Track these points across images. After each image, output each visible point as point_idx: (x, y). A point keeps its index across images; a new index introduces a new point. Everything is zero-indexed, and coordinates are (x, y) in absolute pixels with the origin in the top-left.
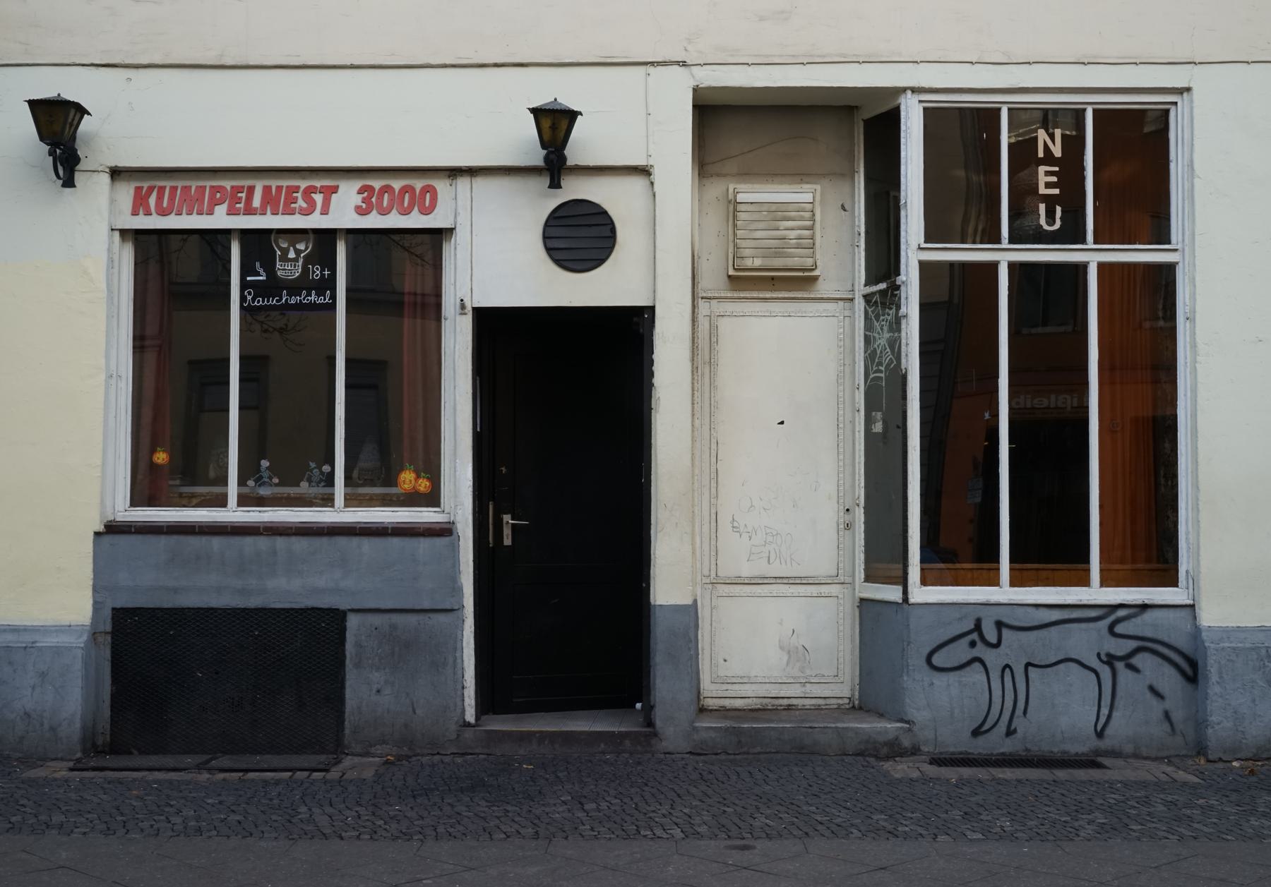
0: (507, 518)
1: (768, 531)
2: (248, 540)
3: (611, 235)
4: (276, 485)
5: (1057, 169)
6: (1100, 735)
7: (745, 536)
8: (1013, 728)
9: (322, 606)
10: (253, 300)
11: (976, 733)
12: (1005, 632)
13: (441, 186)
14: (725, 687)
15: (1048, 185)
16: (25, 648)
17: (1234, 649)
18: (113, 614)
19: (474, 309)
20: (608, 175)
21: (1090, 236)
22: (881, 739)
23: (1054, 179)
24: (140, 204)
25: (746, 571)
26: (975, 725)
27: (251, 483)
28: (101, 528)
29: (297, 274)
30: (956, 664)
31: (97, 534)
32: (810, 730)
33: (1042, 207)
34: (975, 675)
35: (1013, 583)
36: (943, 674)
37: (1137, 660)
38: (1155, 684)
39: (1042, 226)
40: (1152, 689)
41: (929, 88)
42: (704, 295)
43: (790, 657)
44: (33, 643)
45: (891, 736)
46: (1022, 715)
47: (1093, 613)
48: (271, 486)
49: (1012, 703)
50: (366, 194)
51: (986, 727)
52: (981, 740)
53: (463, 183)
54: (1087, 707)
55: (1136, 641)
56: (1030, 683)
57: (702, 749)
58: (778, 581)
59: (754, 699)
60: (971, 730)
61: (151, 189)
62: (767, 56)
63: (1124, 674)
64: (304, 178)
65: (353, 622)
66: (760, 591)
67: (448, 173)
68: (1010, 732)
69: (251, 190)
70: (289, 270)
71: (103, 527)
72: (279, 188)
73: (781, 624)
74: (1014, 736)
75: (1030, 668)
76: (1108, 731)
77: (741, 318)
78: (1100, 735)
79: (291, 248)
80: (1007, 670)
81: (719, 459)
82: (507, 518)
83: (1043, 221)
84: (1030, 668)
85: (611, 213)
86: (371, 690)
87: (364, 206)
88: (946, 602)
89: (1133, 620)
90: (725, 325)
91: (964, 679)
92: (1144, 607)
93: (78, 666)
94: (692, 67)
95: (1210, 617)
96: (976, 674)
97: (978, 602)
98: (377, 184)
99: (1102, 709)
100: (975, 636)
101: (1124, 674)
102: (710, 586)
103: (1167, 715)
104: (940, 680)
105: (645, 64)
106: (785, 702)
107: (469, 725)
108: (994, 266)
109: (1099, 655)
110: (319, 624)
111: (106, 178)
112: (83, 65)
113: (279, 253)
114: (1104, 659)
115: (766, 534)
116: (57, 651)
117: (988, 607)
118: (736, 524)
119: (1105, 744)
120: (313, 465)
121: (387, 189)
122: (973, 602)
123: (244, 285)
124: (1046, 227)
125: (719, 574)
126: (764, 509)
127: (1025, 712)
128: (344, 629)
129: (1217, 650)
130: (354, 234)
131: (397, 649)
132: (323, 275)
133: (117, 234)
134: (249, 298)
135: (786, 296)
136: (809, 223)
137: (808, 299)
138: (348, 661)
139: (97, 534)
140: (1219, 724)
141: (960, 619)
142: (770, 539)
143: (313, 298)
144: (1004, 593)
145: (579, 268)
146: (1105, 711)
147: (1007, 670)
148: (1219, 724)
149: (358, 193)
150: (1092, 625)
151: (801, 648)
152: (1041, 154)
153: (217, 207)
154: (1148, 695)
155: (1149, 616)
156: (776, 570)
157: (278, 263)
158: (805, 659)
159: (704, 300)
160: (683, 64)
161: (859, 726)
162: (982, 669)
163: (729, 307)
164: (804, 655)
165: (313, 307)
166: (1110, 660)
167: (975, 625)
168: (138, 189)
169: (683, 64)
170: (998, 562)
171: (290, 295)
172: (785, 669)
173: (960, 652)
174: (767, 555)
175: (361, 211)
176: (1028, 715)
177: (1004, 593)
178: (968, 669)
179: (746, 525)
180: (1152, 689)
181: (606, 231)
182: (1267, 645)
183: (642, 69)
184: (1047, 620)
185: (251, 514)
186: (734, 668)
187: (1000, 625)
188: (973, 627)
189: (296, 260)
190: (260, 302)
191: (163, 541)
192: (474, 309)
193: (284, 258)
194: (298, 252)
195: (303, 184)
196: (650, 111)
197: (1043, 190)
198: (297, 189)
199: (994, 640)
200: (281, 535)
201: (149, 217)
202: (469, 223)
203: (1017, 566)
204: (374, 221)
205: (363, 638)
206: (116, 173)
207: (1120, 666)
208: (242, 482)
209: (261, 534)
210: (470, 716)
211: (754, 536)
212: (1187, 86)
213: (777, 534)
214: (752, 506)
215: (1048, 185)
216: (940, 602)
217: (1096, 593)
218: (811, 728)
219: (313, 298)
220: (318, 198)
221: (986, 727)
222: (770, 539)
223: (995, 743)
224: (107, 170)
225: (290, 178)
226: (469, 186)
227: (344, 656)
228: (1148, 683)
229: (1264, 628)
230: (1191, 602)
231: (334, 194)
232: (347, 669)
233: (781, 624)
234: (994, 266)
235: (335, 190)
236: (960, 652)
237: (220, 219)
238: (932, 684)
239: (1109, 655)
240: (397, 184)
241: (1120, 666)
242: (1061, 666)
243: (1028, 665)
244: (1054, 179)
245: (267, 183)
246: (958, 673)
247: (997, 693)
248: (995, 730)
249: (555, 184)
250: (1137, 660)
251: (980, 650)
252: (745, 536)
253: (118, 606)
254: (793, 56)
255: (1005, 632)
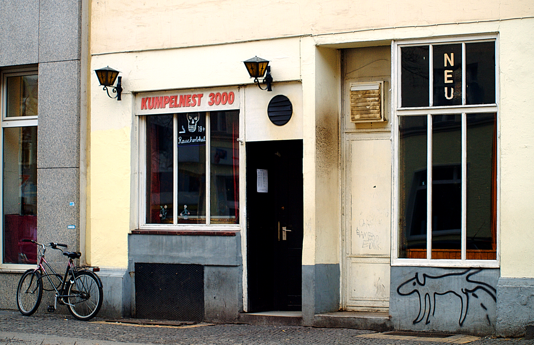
0: (284, 228)
1: (370, 234)
2: (174, 238)
3: (290, 109)
4: (189, 215)
5: (452, 71)
6: (461, 325)
7: (361, 236)
8: (428, 321)
9: (196, 263)
10: (181, 141)
11: (415, 322)
12: (427, 278)
13: (235, 92)
14: (354, 302)
15: (449, 79)
16: (106, 277)
17: (508, 288)
18: (135, 265)
19: (246, 143)
20: (290, 84)
21: (464, 101)
22: (380, 323)
23: (450, 76)
24: (143, 106)
25: (362, 252)
26: (415, 319)
27: (181, 214)
28: (131, 232)
29: (195, 130)
30: (408, 293)
31: (129, 234)
32: (354, 319)
33: (446, 89)
34: (415, 298)
35: (468, 258)
36: (403, 296)
37: (476, 292)
38: (483, 303)
39: (446, 98)
40: (482, 305)
41: (399, 39)
42: (346, 131)
43: (378, 289)
44: (109, 275)
45: (382, 323)
46: (432, 315)
47: (461, 271)
48: (187, 215)
49: (429, 310)
50: (212, 97)
51: (418, 320)
52: (417, 325)
53: (242, 90)
54: (457, 312)
55: (477, 284)
56: (436, 301)
57: (317, 325)
58: (374, 256)
59: (365, 307)
60: (413, 321)
61: (147, 99)
62: (340, 30)
63: (472, 298)
64: (192, 92)
65: (206, 270)
66: (367, 261)
67: (238, 86)
68: (428, 323)
69: (176, 97)
70: (192, 129)
71: (131, 232)
72: (185, 96)
73: (375, 275)
74: (428, 324)
75: (436, 295)
76: (464, 323)
77: (360, 141)
78: (461, 325)
79: (193, 120)
80: (427, 295)
81: (352, 203)
82: (284, 228)
83: (446, 95)
84: (436, 295)
85: (291, 100)
86: (212, 297)
87: (211, 101)
88: (404, 265)
89: (476, 274)
90: (354, 144)
91: (411, 299)
92: (481, 269)
93: (121, 285)
94: (314, 37)
95: (505, 274)
96: (415, 296)
97: (416, 265)
98: (215, 92)
99: (462, 313)
100: (415, 280)
101: (472, 298)
102: (349, 258)
103: (487, 316)
104: (403, 299)
105: (299, 36)
106: (377, 309)
107: (244, 312)
108: (425, 117)
109: (462, 290)
110: (198, 271)
111: (131, 96)
112: (123, 52)
113: (189, 122)
114: (464, 291)
115: (369, 236)
116: (116, 278)
117: (420, 268)
118: (358, 232)
119: (464, 328)
120: (161, 207)
121: (218, 94)
122: (414, 265)
123: (179, 135)
124: (448, 98)
125: (352, 253)
126: (368, 225)
127: (433, 314)
128: (203, 273)
129: (501, 288)
130: (213, 114)
131: (220, 281)
132: (203, 130)
133: (138, 117)
134: (180, 140)
135: (376, 130)
136: (377, 99)
137: (379, 132)
138: (205, 286)
139: (129, 234)
140: (500, 321)
141: (410, 273)
142: (370, 238)
143: (199, 139)
144: (428, 262)
145: (282, 124)
146: (464, 314)
147: (427, 295)
148: (500, 321)
149: (209, 97)
150: (460, 276)
151: (382, 286)
152: (446, 65)
153: (166, 105)
154: (481, 308)
155: (483, 272)
156: (373, 252)
157: (189, 126)
158: (383, 290)
159: (347, 134)
160: (311, 35)
161: (371, 318)
162: (418, 295)
163: (356, 136)
164: (383, 289)
165: (200, 142)
166: (467, 292)
167: (416, 276)
168: (143, 99)
169: (311, 35)
170: (461, 249)
171: (192, 138)
172: (376, 295)
173: (410, 287)
174: (369, 245)
175: (211, 104)
176: (434, 315)
177: (428, 262)
178: (412, 295)
179: (362, 232)
180: (482, 305)
181: (288, 108)
182: (521, 286)
183: (298, 39)
184: (443, 274)
185: (180, 227)
186: (357, 294)
187: (425, 276)
188: (415, 276)
189: (194, 124)
190: (183, 142)
191: (149, 237)
192: (246, 143)
193: (191, 124)
194: (195, 121)
195: (192, 94)
196: (301, 57)
197: (446, 81)
198: (190, 96)
199: (423, 283)
200: (183, 235)
201: (146, 110)
202: (244, 107)
203: (435, 250)
204: (215, 108)
205: (210, 276)
206: (135, 94)
207: (470, 294)
208: (179, 214)
209: (177, 235)
210: (245, 309)
211: (364, 237)
212: (497, 31)
213: (373, 236)
214: (364, 223)
215: (449, 79)
216: (402, 265)
217: (464, 262)
218: (354, 318)
219: (199, 139)
220: (197, 99)
221: (418, 320)
222: (370, 238)
223: (421, 327)
224: (131, 93)
225: (185, 92)
226: (244, 92)
227: (203, 284)
228: (480, 303)
229: (525, 279)
230: (499, 267)
231: (202, 98)
232: (205, 289)
233: (375, 275)
234: (425, 117)
235: (202, 96)
236: (410, 287)
237: (167, 110)
238: (399, 301)
239: (466, 290)
240: (221, 92)
241: (470, 294)
242: (448, 294)
243: (435, 293)
244: (450, 76)
245: (181, 94)
246: (409, 296)
247: (423, 305)
248: (422, 321)
249: (270, 90)
250: (476, 292)
251: (417, 287)
252: (361, 236)
253: (136, 262)
254: (350, 29)
255: (427, 278)
